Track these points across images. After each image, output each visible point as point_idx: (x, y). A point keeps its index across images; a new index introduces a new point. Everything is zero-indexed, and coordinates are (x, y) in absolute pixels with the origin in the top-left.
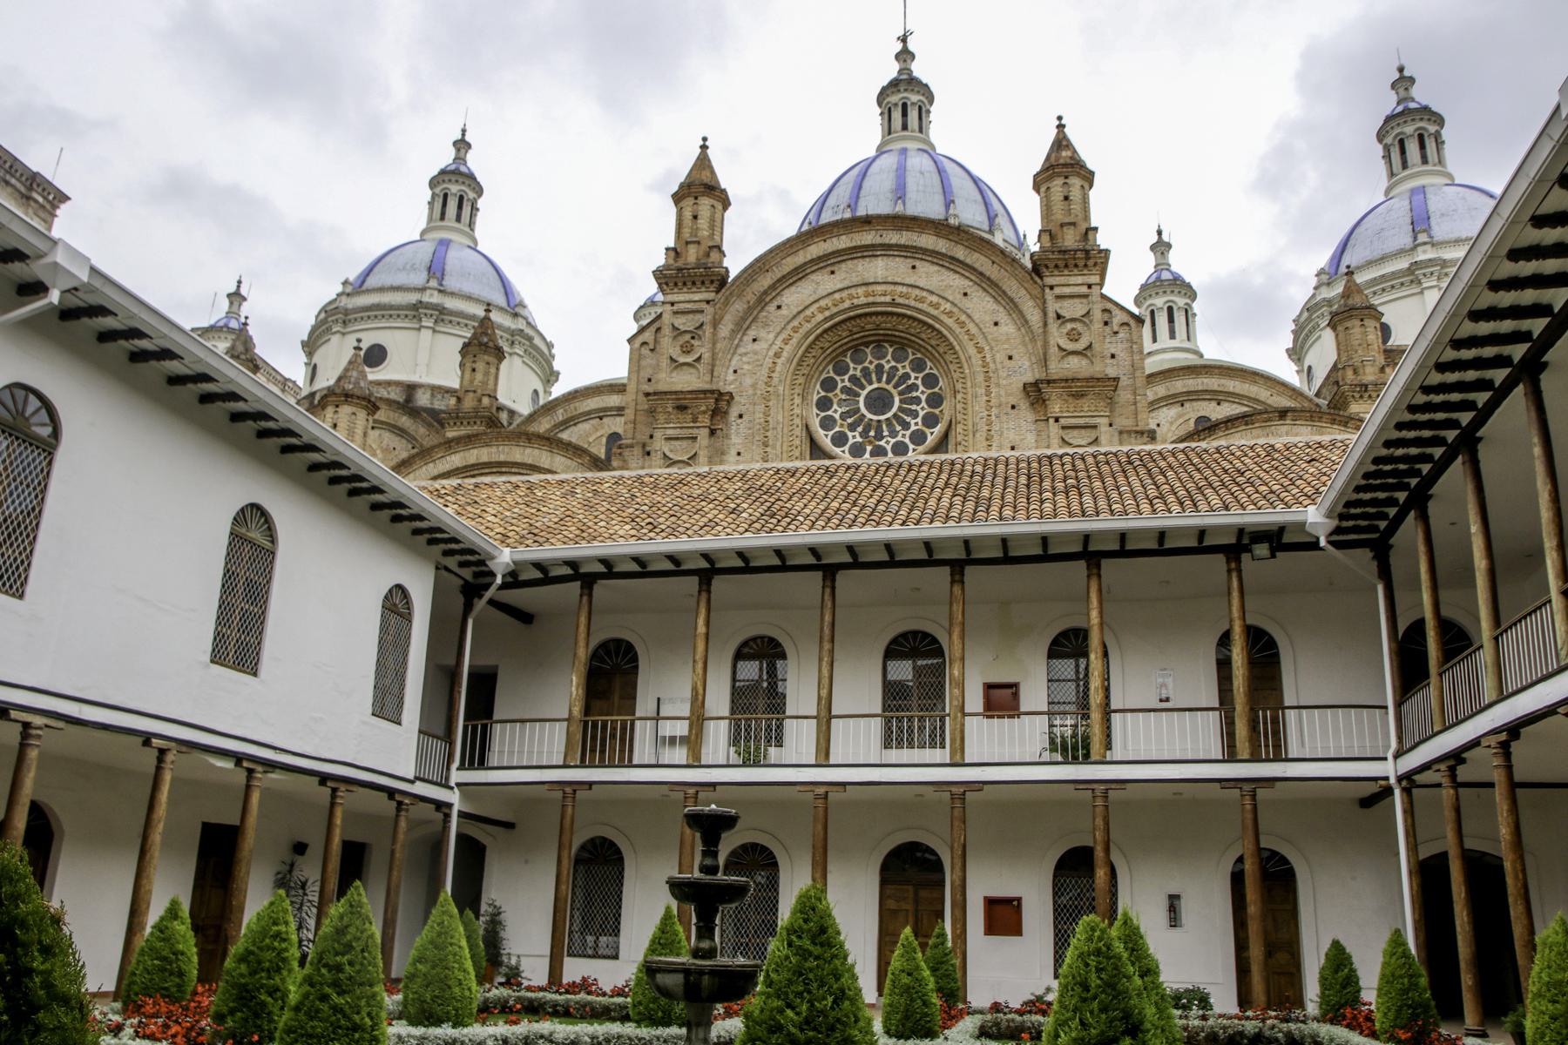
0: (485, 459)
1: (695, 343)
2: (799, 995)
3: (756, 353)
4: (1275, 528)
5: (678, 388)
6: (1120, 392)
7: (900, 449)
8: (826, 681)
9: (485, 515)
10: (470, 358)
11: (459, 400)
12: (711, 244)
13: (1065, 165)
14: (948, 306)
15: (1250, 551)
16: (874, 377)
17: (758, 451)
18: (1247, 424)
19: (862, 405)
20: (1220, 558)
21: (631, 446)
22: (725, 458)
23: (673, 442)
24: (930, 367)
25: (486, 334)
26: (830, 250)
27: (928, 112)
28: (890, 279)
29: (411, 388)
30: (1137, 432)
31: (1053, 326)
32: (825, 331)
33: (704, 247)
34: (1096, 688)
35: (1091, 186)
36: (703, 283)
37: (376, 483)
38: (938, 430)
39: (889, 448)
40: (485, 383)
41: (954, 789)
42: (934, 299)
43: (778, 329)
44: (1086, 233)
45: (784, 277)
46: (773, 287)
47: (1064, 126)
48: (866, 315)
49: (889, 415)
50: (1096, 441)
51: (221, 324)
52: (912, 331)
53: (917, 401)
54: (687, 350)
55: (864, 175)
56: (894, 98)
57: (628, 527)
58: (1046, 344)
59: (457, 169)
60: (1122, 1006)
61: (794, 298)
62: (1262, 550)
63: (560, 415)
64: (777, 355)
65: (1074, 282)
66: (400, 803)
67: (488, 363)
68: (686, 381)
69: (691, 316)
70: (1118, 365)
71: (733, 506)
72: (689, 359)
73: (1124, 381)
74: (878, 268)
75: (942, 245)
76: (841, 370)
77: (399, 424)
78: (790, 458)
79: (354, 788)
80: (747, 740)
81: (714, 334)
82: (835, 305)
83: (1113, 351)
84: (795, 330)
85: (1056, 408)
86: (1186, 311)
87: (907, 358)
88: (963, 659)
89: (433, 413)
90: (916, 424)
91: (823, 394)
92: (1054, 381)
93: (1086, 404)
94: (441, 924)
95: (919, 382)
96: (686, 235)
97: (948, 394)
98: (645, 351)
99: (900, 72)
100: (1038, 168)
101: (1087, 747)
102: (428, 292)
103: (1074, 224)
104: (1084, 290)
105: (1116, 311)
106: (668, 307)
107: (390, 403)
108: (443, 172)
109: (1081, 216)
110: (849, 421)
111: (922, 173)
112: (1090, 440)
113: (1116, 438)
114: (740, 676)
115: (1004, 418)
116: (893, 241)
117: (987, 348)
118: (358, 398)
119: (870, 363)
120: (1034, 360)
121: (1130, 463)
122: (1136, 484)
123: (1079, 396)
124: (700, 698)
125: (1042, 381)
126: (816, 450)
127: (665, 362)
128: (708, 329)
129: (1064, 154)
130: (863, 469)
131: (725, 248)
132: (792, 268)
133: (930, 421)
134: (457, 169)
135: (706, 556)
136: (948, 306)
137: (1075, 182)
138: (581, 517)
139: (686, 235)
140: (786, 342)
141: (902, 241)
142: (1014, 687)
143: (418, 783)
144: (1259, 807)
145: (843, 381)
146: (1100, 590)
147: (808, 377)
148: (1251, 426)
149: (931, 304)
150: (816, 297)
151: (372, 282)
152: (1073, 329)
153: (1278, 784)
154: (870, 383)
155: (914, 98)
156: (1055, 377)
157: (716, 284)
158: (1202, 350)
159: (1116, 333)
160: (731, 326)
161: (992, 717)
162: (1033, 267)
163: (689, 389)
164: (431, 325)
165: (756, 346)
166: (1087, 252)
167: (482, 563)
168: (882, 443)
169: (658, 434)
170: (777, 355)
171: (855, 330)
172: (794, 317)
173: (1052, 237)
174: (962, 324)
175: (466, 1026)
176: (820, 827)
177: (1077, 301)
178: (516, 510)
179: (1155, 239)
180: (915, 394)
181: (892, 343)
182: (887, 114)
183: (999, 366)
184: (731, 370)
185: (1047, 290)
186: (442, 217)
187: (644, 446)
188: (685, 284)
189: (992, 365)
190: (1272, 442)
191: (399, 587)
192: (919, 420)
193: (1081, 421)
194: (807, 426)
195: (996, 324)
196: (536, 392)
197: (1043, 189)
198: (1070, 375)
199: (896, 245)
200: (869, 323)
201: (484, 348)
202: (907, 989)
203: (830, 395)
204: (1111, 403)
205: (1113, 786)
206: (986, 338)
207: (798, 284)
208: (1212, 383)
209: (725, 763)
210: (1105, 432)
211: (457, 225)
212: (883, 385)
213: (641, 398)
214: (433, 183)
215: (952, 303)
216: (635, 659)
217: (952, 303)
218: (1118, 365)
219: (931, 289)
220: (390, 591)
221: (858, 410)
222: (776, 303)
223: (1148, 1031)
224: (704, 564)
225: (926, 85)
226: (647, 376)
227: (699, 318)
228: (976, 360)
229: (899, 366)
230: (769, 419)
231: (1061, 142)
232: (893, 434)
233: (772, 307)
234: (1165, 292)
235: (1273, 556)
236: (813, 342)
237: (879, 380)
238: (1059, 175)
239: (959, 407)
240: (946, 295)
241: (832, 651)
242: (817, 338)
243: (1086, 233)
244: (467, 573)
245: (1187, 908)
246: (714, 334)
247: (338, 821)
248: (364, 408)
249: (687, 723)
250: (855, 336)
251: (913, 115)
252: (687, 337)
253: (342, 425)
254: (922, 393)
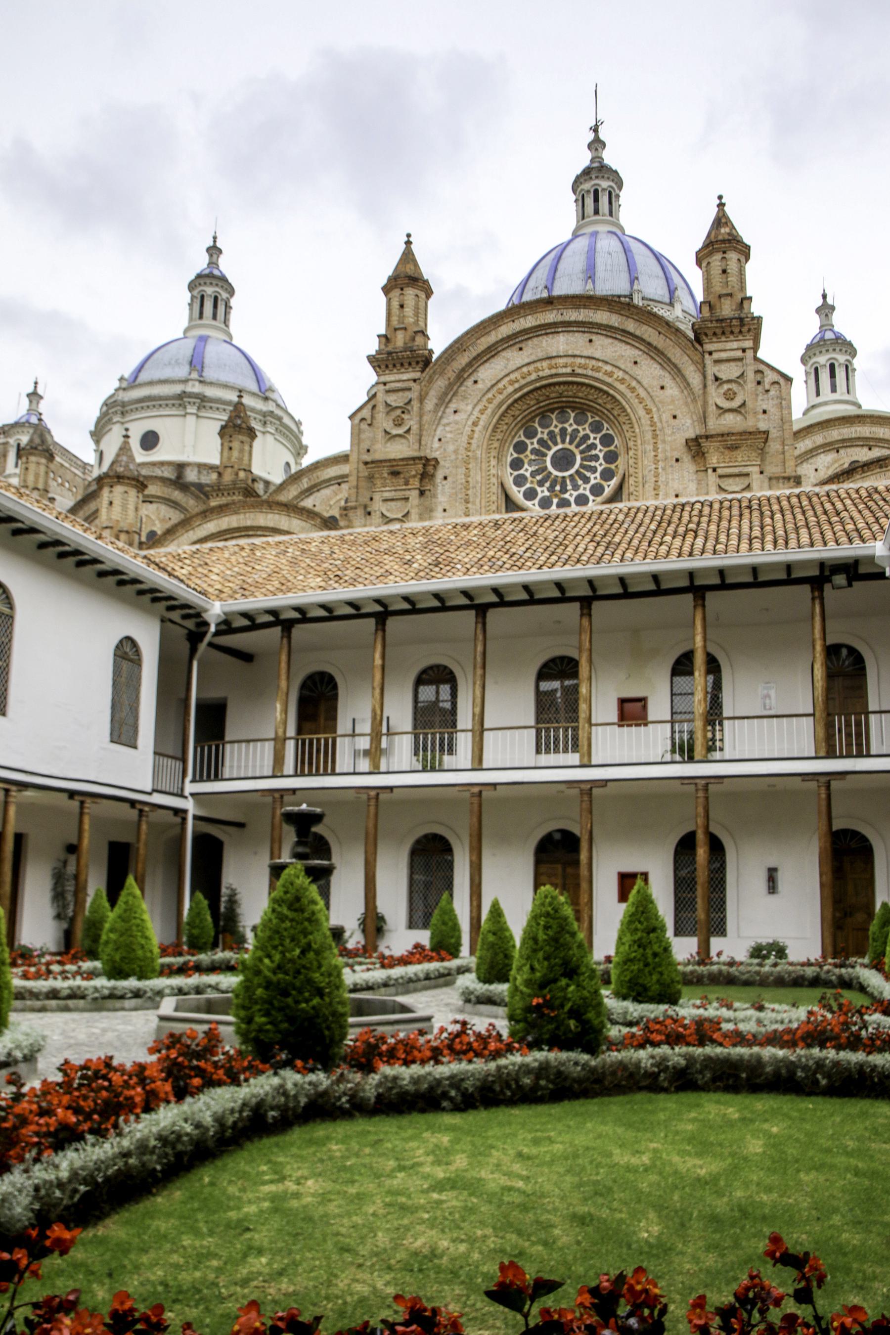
0: (235, 525)
1: (405, 416)
2: (275, 947)
3: (457, 423)
4: (851, 561)
5: (392, 456)
6: (770, 443)
7: (582, 500)
8: (478, 701)
9: (210, 574)
10: (227, 438)
11: (220, 474)
12: (416, 329)
13: (723, 241)
14: (621, 374)
15: (830, 581)
16: (559, 439)
17: (461, 508)
18: (881, 467)
19: (549, 464)
20: (807, 588)
21: (355, 508)
22: (434, 514)
23: (389, 503)
24: (606, 429)
25: (239, 417)
26: (518, 329)
27: (618, 196)
28: (570, 353)
29: (180, 467)
30: (784, 478)
31: (712, 387)
32: (516, 401)
33: (410, 333)
34: (699, 701)
35: (747, 258)
36: (410, 364)
37: (94, 555)
38: (614, 483)
39: (572, 500)
40: (240, 459)
41: (583, 786)
42: (609, 368)
43: (475, 401)
44: (742, 302)
45: (479, 355)
46: (470, 364)
47: (724, 205)
48: (550, 385)
49: (572, 471)
50: (748, 487)
51: (23, 420)
52: (591, 397)
53: (596, 458)
54: (398, 423)
55: (559, 258)
56: (587, 186)
57: (319, 579)
58: (705, 404)
59: (211, 273)
60: (562, 955)
61: (488, 373)
62: (840, 579)
63: (305, 483)
64: (475, 424)
65: (731, 347)
66: (141, 811)
67: (242, 442)
68: (399, 450)
69: (401, 394)
70: (769, 419)
71: (408, 557)
72: (400, 431)
73: (774, 434)
74: (560, 343)
75: (614, 320)
76: (530, 434)
77: (173, 498)
78: (488, 512)
79: (99, 800)
80: (425, 749)
81: (421, 409)
82: (523, 378)
83: (765, 407)
84: (490, 401)
85: (713, 459)
86: (847, 367)
87: (586, 421)
88: (590, 678)
89: (200, 487)
90: (595, 478)
91: (515, 455)
92: (712, 436)
93: (740, 456)
94: (126, 903)
95: (597, 442)
96: (395, 323)
97: (622, 451)
98: (364, 426)
99: (592, 161)
100: (699, 245)
101: (691, 750)
102: (190, 383)
103: (731, 295)
104: (739, 354)
105: (767, 372)
106: (381, 387)
107: (163, 480)
108: (199, 276)
109: (737, 287)
110: (539, 478)
111: (610, 254)
112: (744, 486)
113: (766, 484)
114: (422, 697)
115: (670, 470)
116: (573, 319)
117: (654, 410)
118: (128, 478)
119: (556, 426)
120: (695, 418)
121: (749, 507)
122: (779, 525)
123: (733, 448)
124: (378, 718)
125: (701, 437)
126: (511, 505)
127: (380, 435)
128: (415, 404)
129: (723, 230)
130: (526, 521)
131: (429, 332)
132: (486, 346)
133: (607, 475)
134: (211, 273)
135: (378, 601)
136: (621, 374)
137: (733, 256)
138: (285, 572)
139: (395, 323)
140: (482, 412)
141: (580, 318)
142: (643, 700)
143: (155, 795)
144: (710, 799)
145: (532, 443)
146: (704, 619)
147: (502, 442)
149: (606, 373)
150: (507, 372)
151: (144, 377)
152: (729, 389)
153: (849, 777)
154: (556, 444)
155: (605, 184)
156: (713, 432)
157: (421, 365)
158: (861, 401)
159: (767, 391)
160: (435, 401)
161: (623, 726)
162: (695, 336)
163: (401, 457)
164: (194, 411)
165: (457, 417)
166: (741, 320)
167: (198, 615)
168: (566, 496)
169: (377, 497)
170: (475, 424)
171: (541, 399)
172: (489, 390)
173: (711, 307)
174: (633, 390)
175: (150, 978)
176: (475, 820)
177: (732, 364)
178: (236, 569)
179: (820, 302)
180: (593, 452)
181: (573, 409)
182: (581, 201)
183: (665, 425)
184: (436, 439)
185: (707, 356)
186: (201, 316)
187: (365, 507)
188: (394, 366)
189: (658, 424)
190: (875, 485)
191: (128, 638)
192: (598, 475)
193: (736, 470)
194: (502, 484)
195: (662, 388)
196: (288, 464)
197: (704, 265)
198: (726, 430)
199: (575, 322)
200: (553, 392)
201: (238, 429)
202: (492, 945)
203: (522, 456)
204: (762, 453)
205: (712, 781)
206: (653, 400)
207: (492, 360)
208: (864, 431)
209: (352, 771)
210: (756, 478)
211: (213, 323)
212: (567, 446)
213: (362, 466)
214: (192, 286)
215: (624, 371)
216: (335, 687)
217: (624, 371)
218: (769, 419)
219: (606, 359)
220: (121, 642)
221: (546, 468)
222: (472, 379)
223: (583, 974)
224: (378, 608)
225: (616, 172)
226: (366, 447)
227: (408, 395)
228: (645, 420)
229: (580, 428)
230: (470, 479)
231: (721, 220)
232: (576, 487)
233: (469, 382)
234: (827, 351)
235: (850, 585)
236: (506, 411)
237: (563, 442)
238: (718, 250)
239: (631, 462)
240: (618, 364)
241: (484, 676)
242: (509, 408)
243: (742, 302)
244: (190, 624)
245: (782, 878)
246: (421, 409)
247: (86, 827)
248: (136, 487)
249: (368, 738)
251: (604, 200)
252: (398, 412)
253: (117, 502)
254: (600, 451)
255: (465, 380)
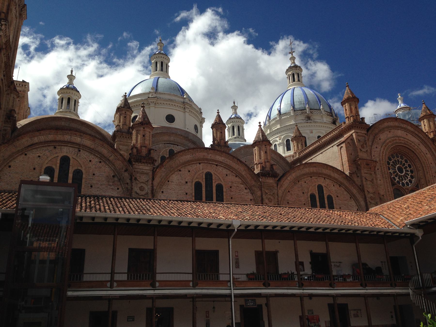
149: (413, 146)
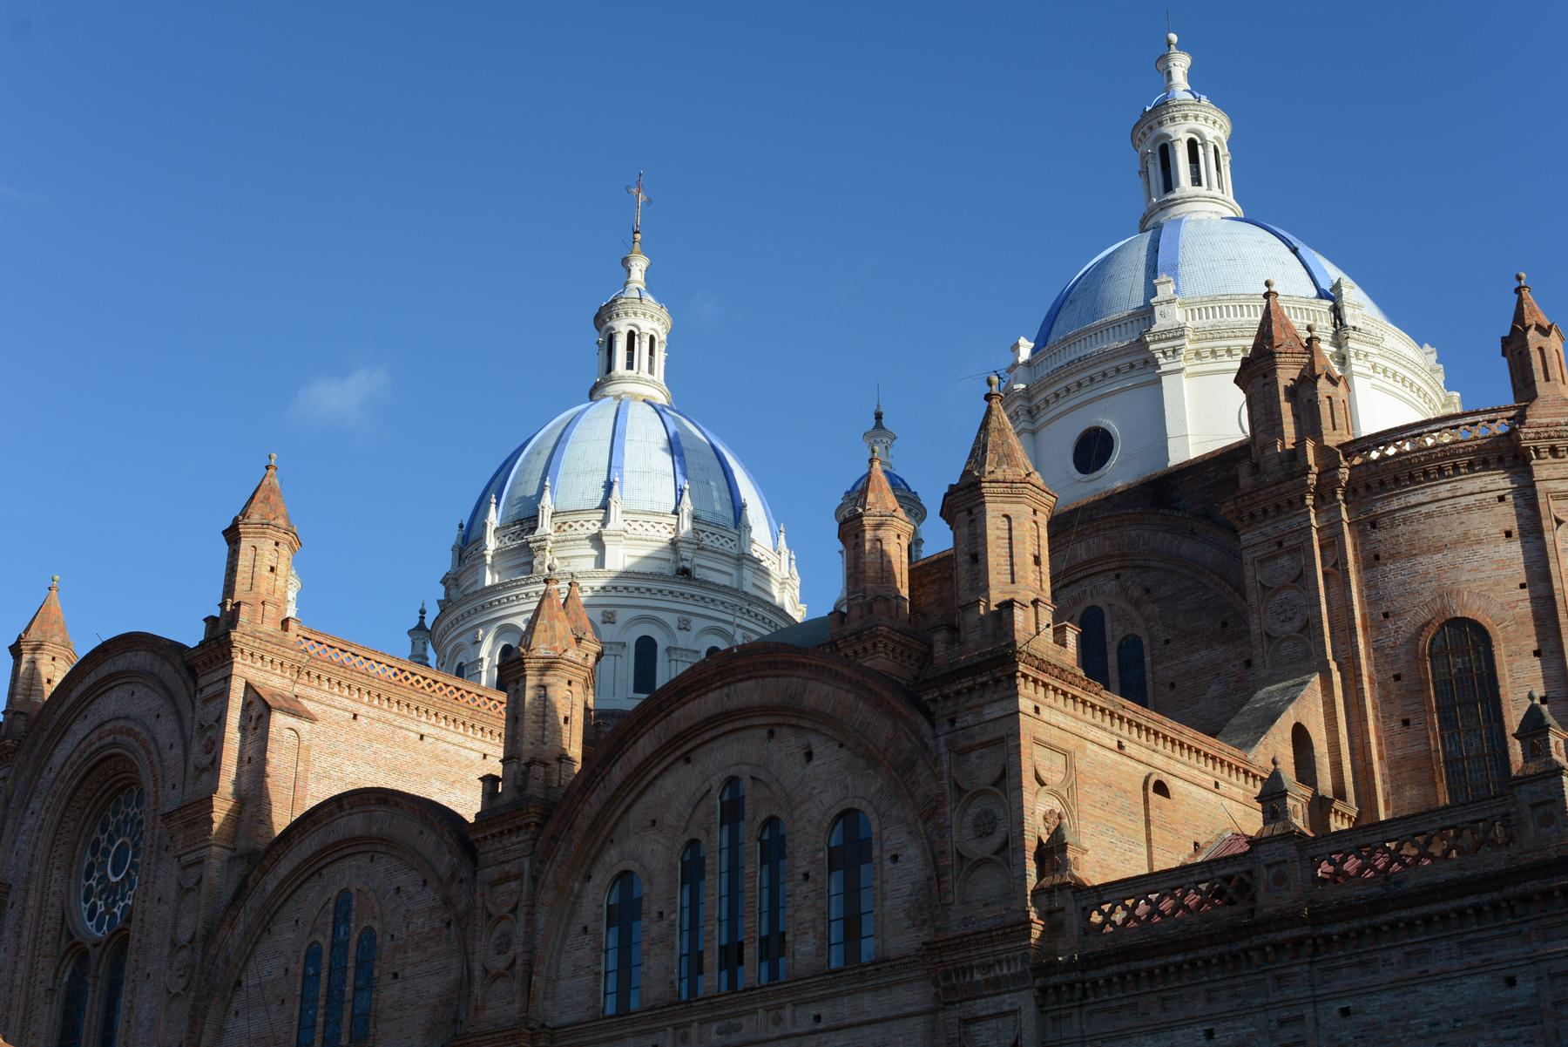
148: (320, 825)
250: (105, 787)
255: (42, 769)
